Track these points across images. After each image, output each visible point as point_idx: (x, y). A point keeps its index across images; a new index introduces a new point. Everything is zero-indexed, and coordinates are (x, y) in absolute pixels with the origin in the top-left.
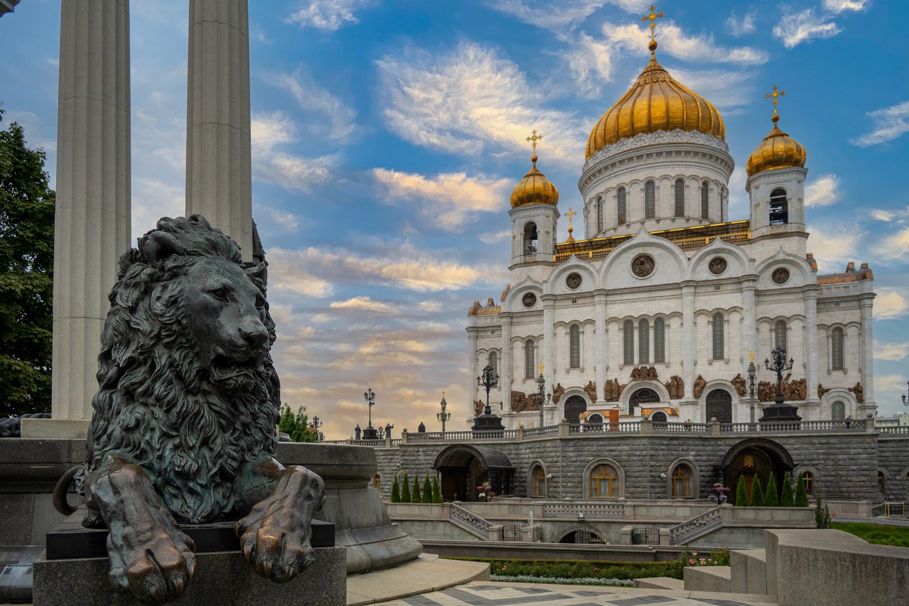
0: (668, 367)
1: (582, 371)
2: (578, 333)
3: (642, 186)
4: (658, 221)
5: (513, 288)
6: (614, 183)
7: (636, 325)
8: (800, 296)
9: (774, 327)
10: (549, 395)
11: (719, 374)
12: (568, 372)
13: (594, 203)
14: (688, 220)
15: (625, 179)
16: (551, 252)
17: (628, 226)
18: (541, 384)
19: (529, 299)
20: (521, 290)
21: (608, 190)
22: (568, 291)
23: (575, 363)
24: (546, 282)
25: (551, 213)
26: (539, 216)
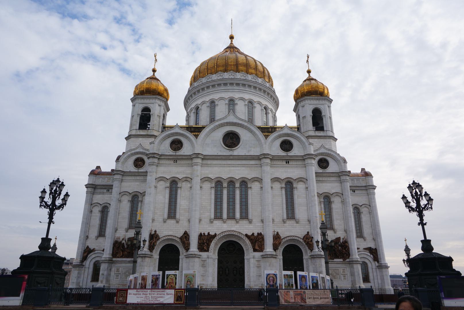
0: (250, 222)
3: (227, 102)
5: (127, 152)
6: (207, 99)
7: (225, 185)
8: (338, 179)
9: (322, 200)
10: (144, 241)
11: (292, 231)
12: (165, 222)
13: (193, 111)
16: (160, 131)
18: (138, 230)
19: (139, 163)
20: (133, 155)
21: (203, 103)
22: (171, 152)
23: (172, 214)
25: (163, 104)
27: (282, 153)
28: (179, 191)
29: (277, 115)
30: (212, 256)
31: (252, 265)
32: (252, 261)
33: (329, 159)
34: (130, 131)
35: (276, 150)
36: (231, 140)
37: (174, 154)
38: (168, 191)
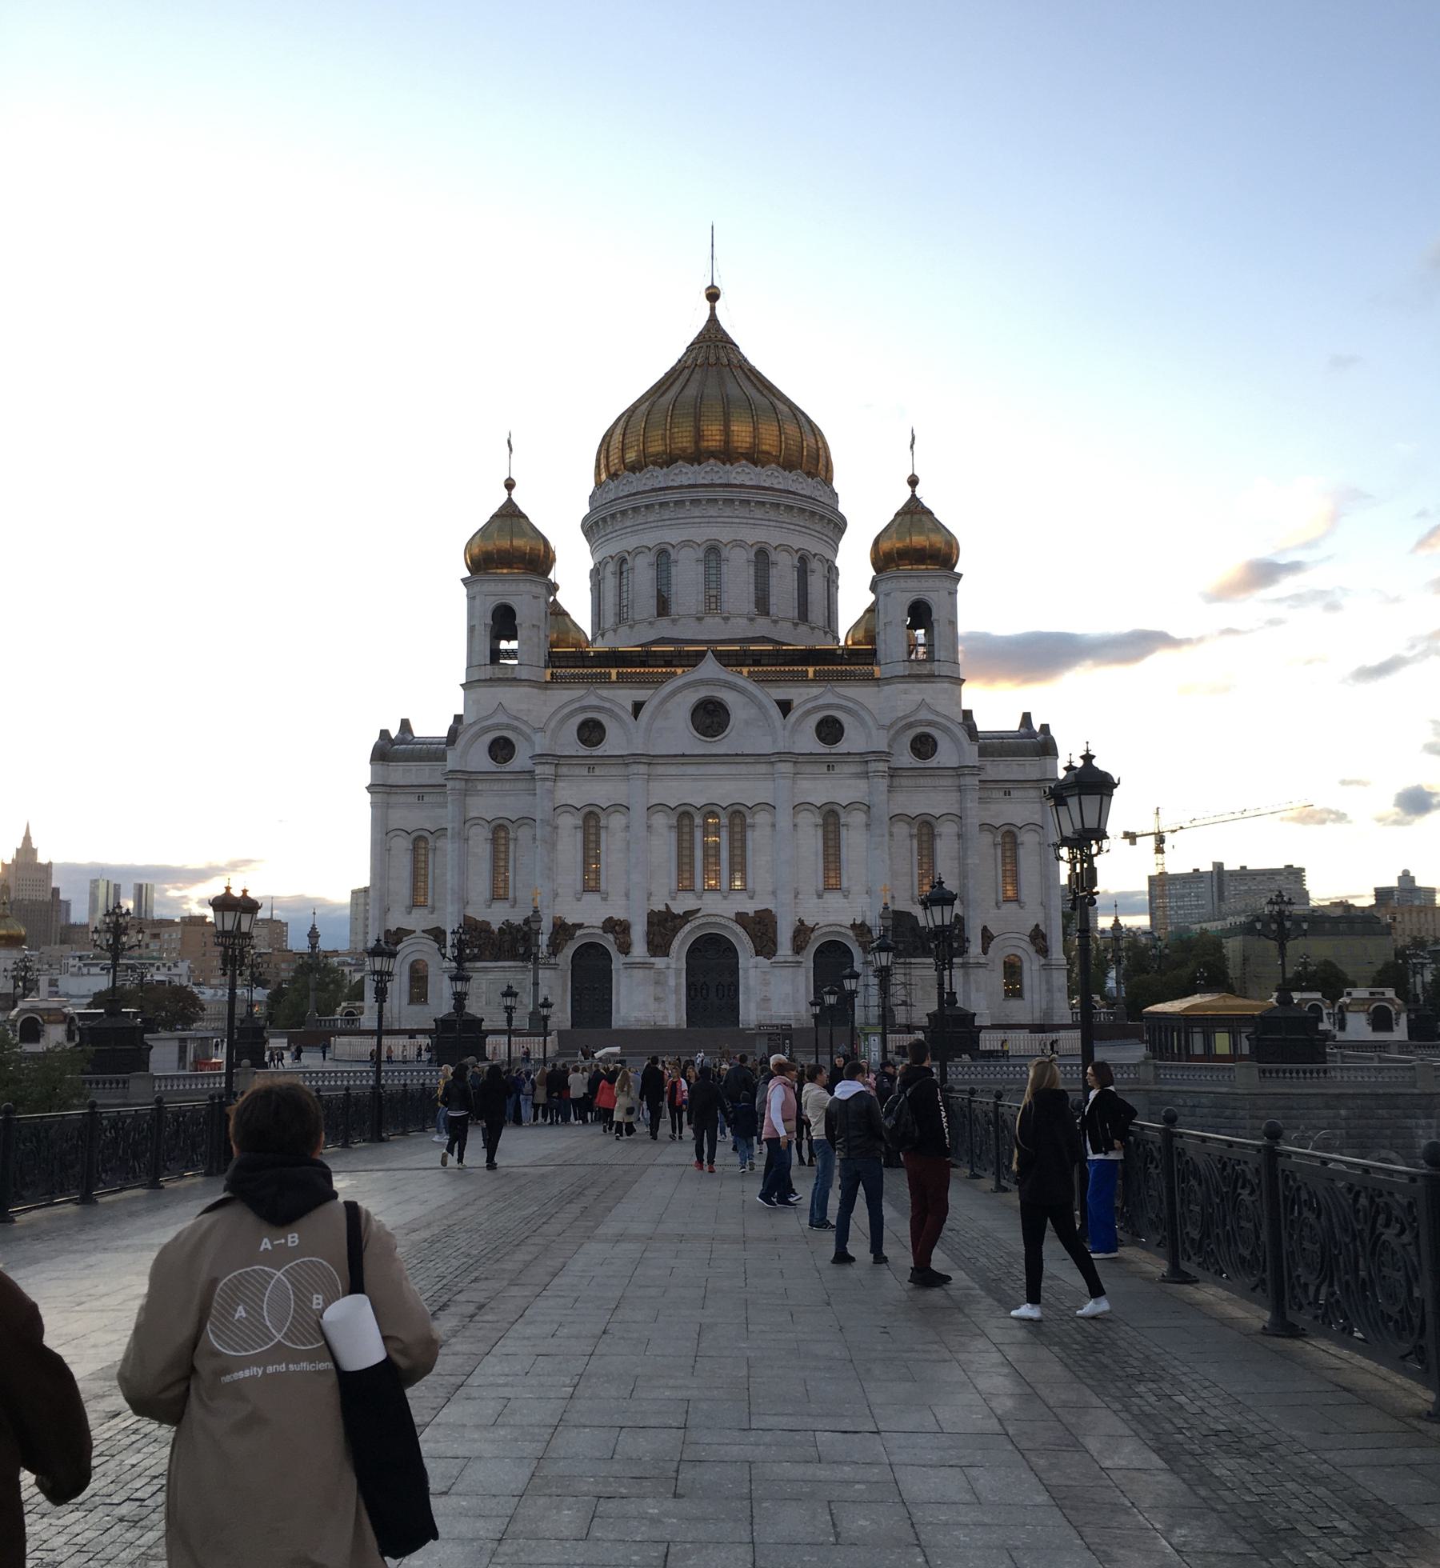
1: (605, 899)
2: (598, 828)
3: (701, 555)
4: (726, 619)
7: (698, 821)
9: (915, 831)
11: (835, 914)
13: (611, 567)
14: (775, 622)
15: (672, 536)
17: (674, 621)
19: (501, 749)
20: (486, 730)
22: (583, 750)
24: (541, 730)
26: (519, 594)
27: (820, 748)
29: (839, 562)
30: (674, 965)
31: (752, 982)
32: (752, 972)
33: (936, 733)
34: (469, 667)
35: (808, 742)
36: (710, 717)
37: (587, 753)
38: (580, 835)
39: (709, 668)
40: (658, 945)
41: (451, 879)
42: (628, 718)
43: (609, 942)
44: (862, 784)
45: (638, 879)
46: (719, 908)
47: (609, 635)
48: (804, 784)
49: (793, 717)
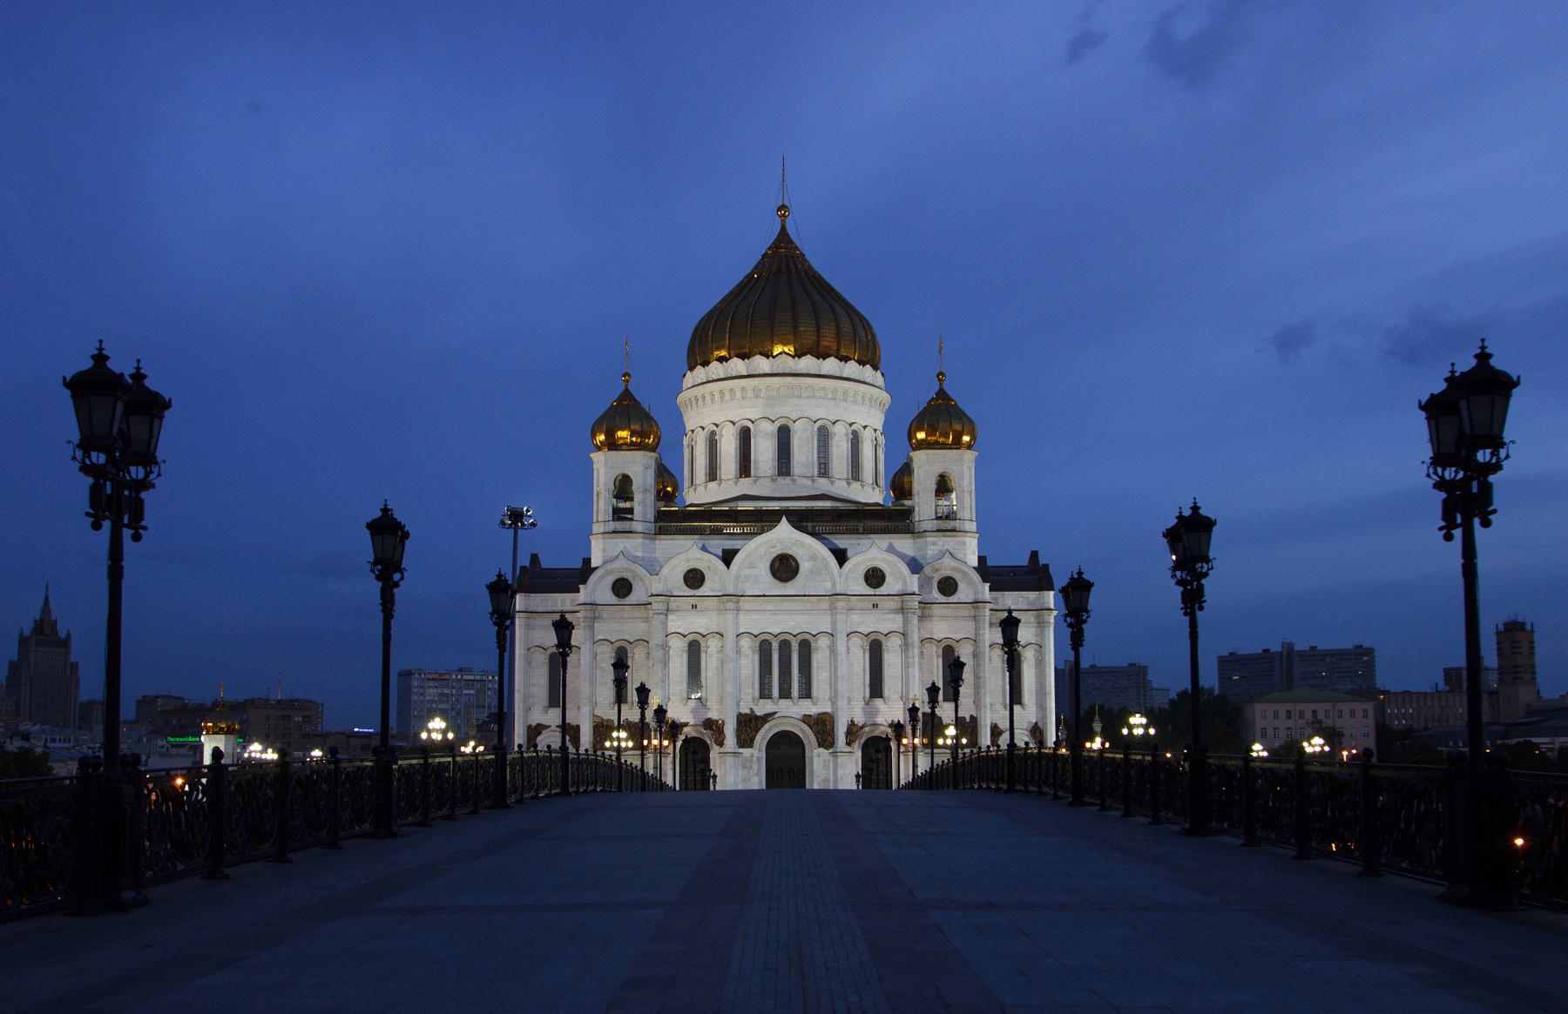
3: (773, 428)
7: (775, 646)
19: (622, 588)
28: (703, 656)
33: (957, 577)
36: (784, 568)
39: (784, 527)
40: (745, 740)
41: (585, 690)
42: (722, 565)
43: (707, 736)
44: (899, 618)
45: (731, 688)
46: (790, 713)
47: (701, 489)
48: (855, 617)
49: (847, 566)
